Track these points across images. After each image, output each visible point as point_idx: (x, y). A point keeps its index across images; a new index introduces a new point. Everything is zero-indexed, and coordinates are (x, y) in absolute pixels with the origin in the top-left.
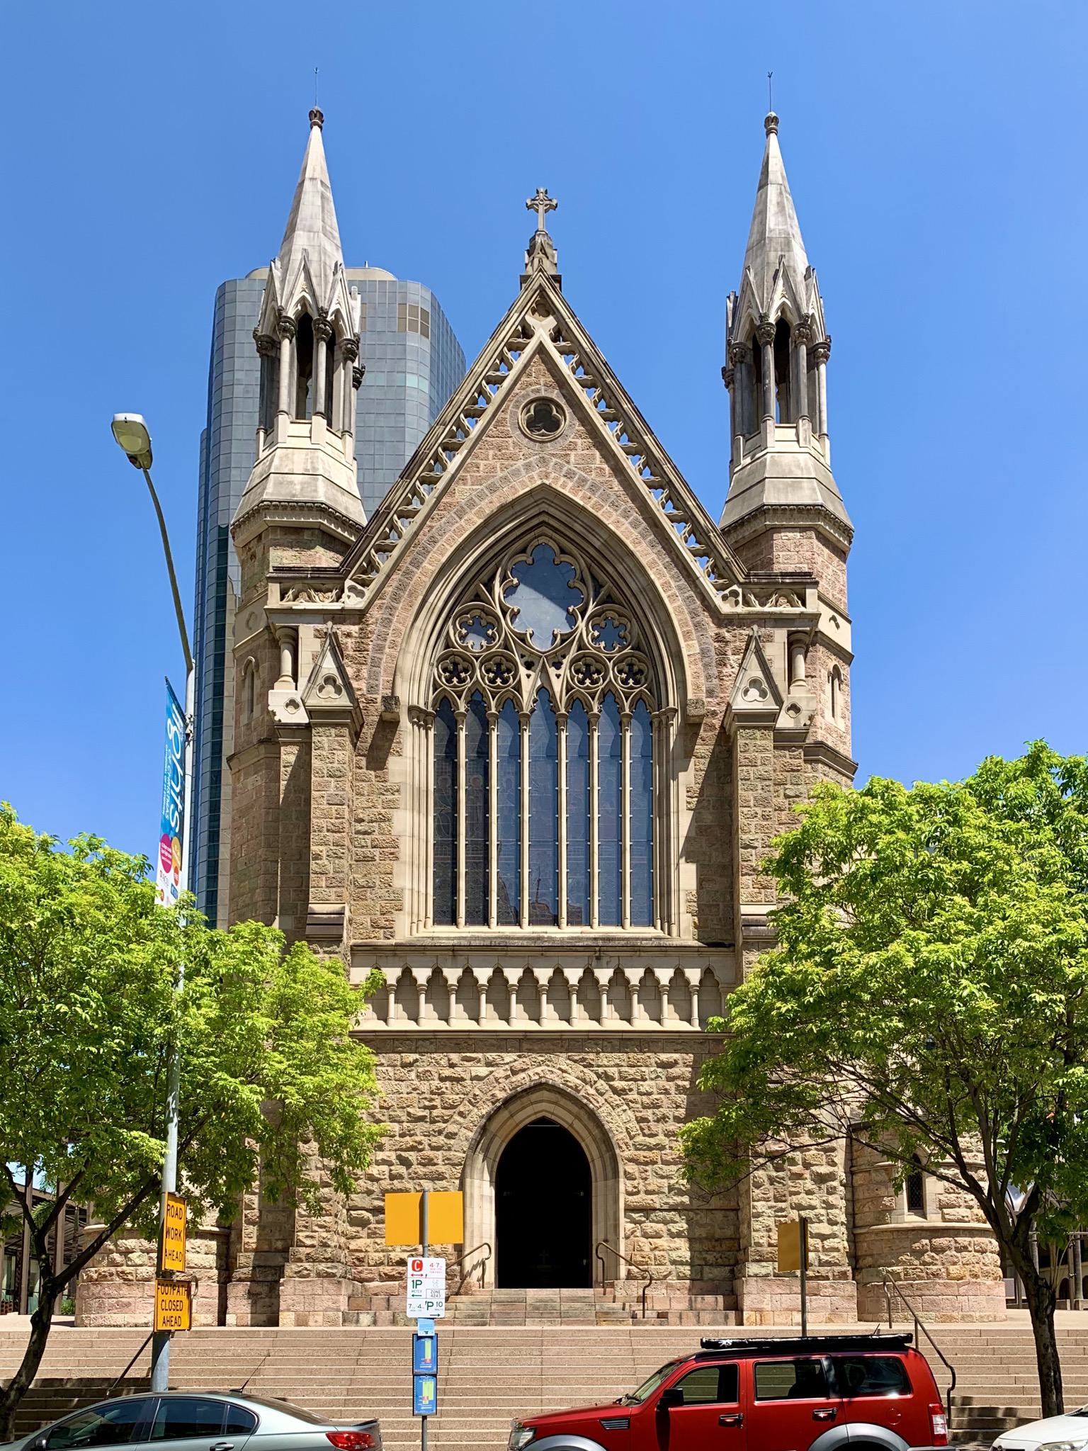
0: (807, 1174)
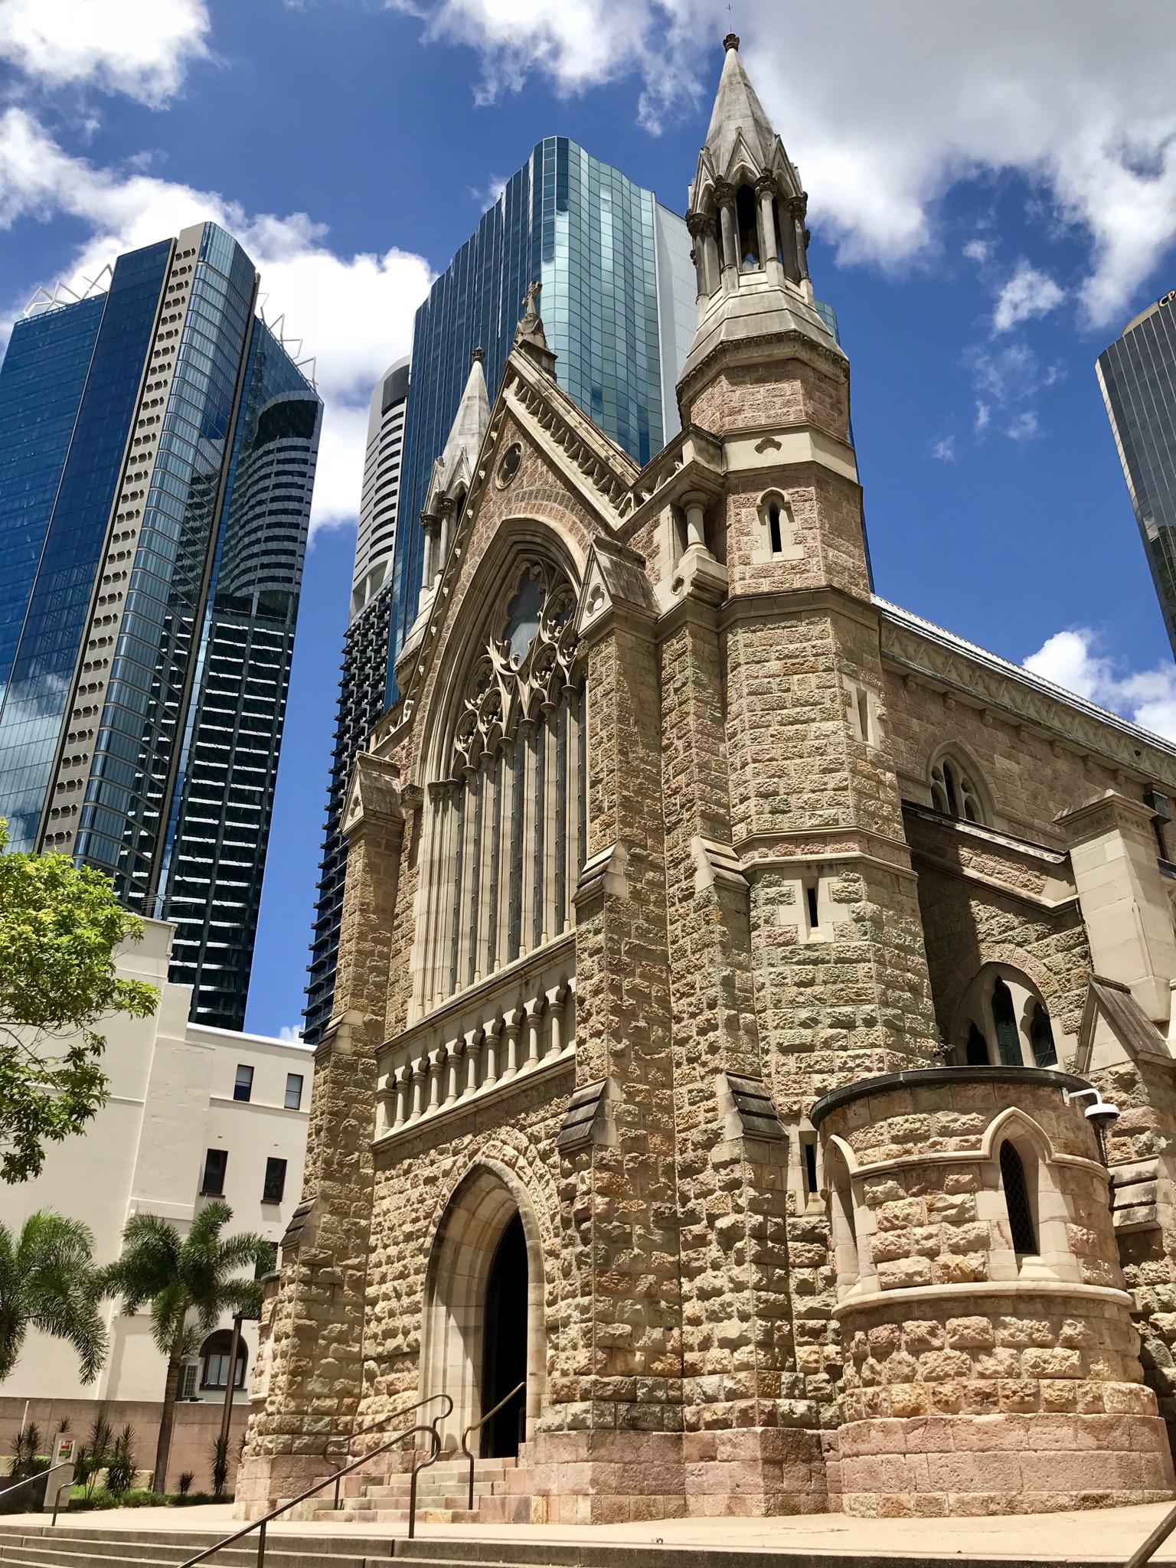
0: (712, 1236)
